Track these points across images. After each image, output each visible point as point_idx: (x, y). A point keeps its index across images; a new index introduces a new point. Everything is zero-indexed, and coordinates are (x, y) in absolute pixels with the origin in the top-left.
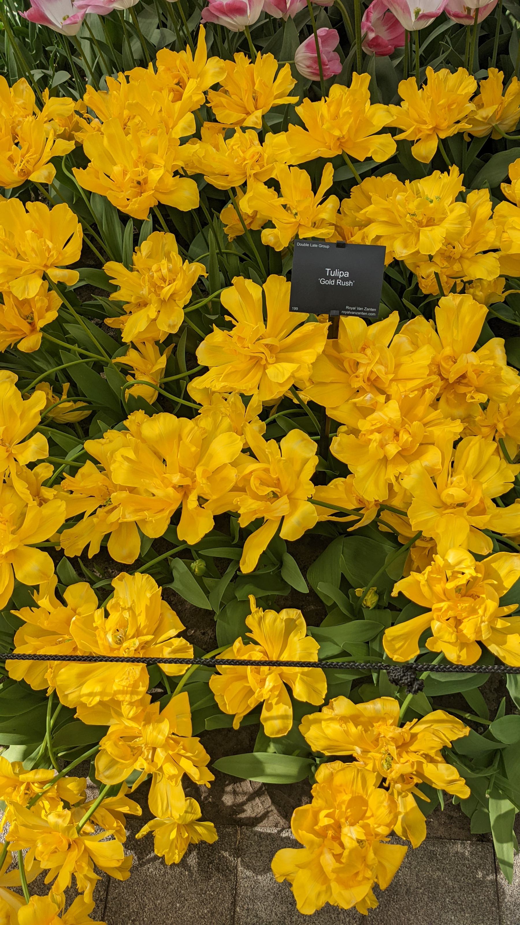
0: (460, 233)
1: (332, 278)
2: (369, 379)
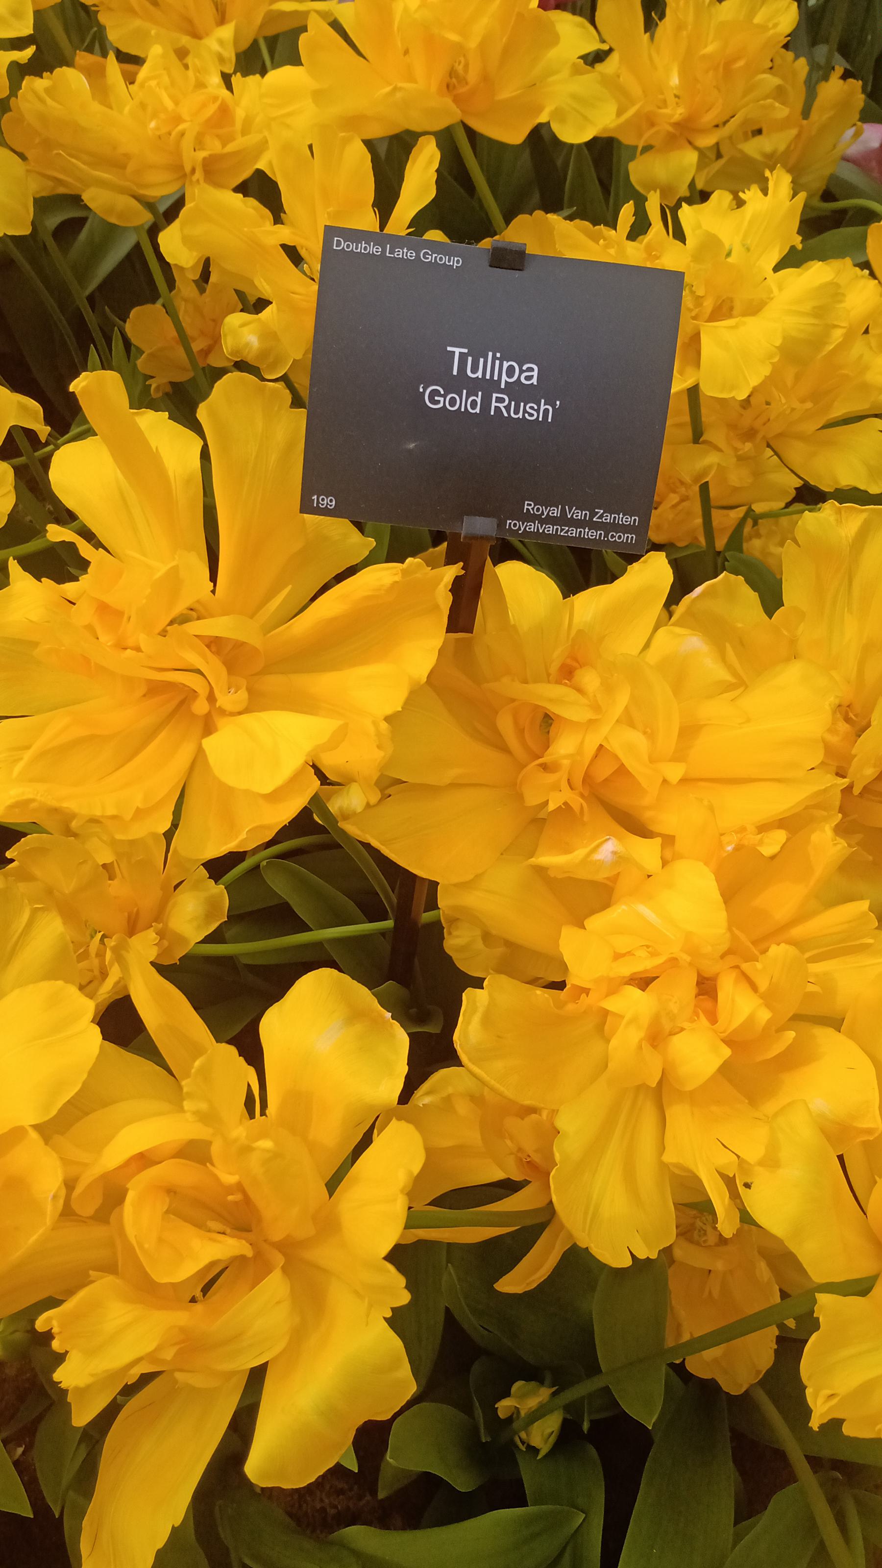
0: (817, 341)
1: (473, 386)
2: (587, 779)
